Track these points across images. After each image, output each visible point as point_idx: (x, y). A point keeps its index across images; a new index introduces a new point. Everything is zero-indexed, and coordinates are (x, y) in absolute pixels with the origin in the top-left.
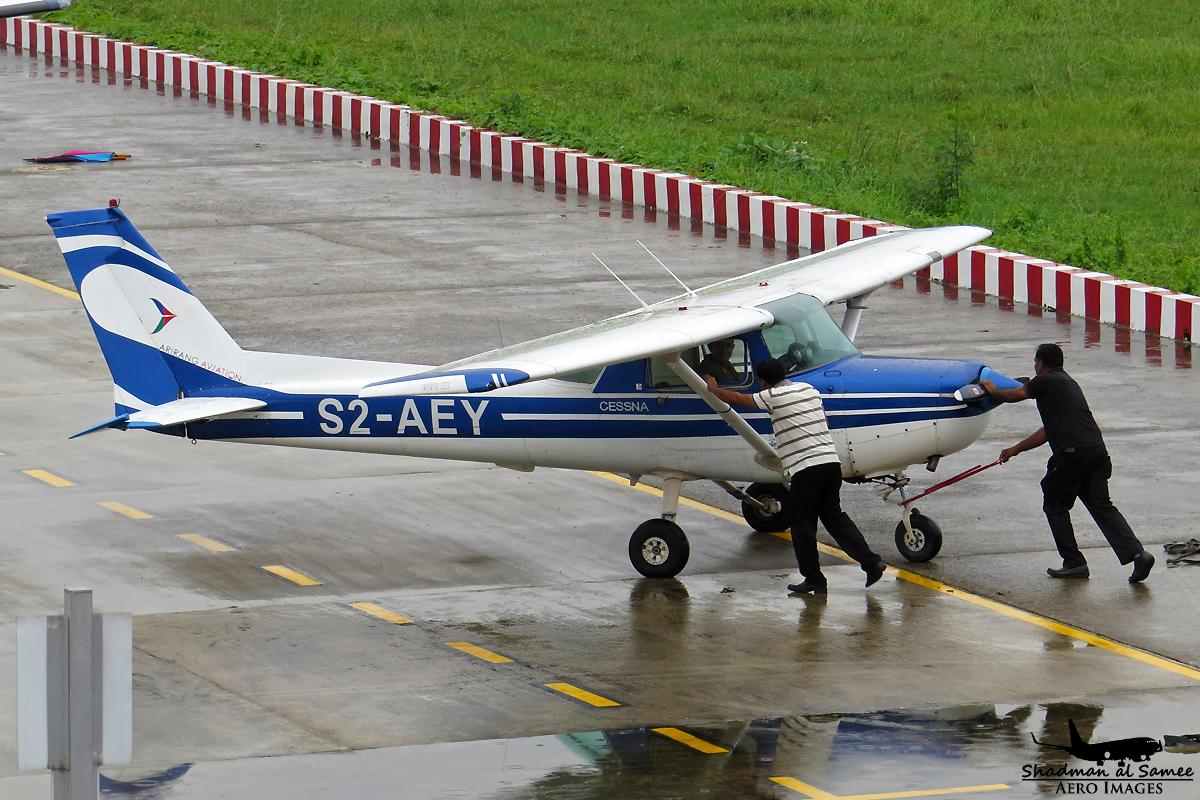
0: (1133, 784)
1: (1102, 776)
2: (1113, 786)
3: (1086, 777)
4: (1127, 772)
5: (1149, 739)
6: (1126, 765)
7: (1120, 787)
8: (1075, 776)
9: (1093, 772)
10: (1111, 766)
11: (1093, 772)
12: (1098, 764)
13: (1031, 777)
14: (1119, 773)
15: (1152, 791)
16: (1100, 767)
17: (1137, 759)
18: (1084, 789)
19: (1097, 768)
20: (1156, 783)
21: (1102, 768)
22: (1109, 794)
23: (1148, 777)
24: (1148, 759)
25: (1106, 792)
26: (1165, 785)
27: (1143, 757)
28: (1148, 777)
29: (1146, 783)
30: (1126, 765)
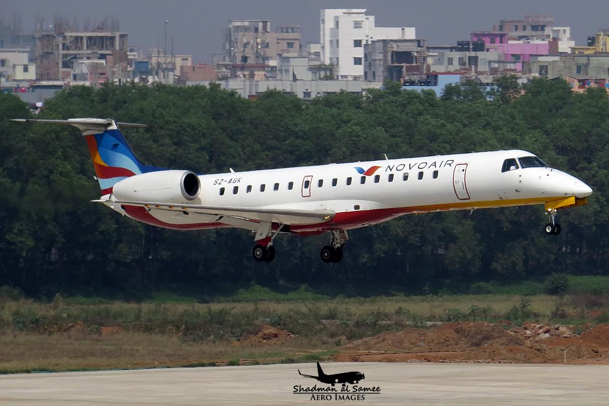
1: (334, 392)
2: (340, 396)
3: (326, 392)
4: (347, 389)
6: (346, 386)
8: (320, 391)
9: (329, 390)
10: (338, 386)
11: (329, 390)
12: (332, 385)
13: (298, 392)
15: (359, 399)
16: (333, 387)
17: (352, 383)
18: (325, 398)
20: (362, 394)
21: (334, 387)
23: (357, 392)
24: (357, 383)
25: (336, 399)
27: (355, 382)
28: (357, 392)
29: (356, 395)
30: (346, 386)
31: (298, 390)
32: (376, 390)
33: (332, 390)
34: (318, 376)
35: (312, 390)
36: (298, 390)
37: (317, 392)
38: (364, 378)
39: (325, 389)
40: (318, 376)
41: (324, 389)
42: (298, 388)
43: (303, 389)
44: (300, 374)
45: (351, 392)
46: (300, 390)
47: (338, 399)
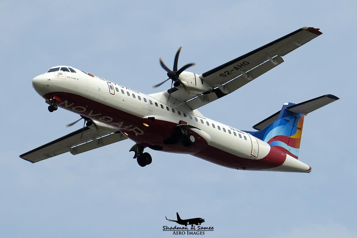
0: (196, 232)
1: (186, 230)
2: (190, 232)
3: (182, 230)
5: (201, 218)
6: (194, 226)
7: (192, 233)
8: (178, 230)
10: (189, 227)
13: (166, 230)
14: (192, 229)
15: (201, 234)
17: (197, 224)
18: (181, 233)
19: (185, 227)
20: (203, 231)
21: (186, 227)
23: (200, 230)
24: (200, 224)
25: (188, 234)
26: (205, 232)
27: (199, 224)
28: (200, 230)
29: (200, 231)
30: (194, 226)
31: (165, 229)
32: (211, 229)
34: (177, 220)
35: (173, 229)
36: (165, 229)
37: (177, 230)
38: (204, 222)
39: (181, 228)
40: (177, 220)
41: (180, 228)
42: (166, 228)
43: (168, 228)
44: (167, 219)
46: (167, 229)
47: (189, 234)
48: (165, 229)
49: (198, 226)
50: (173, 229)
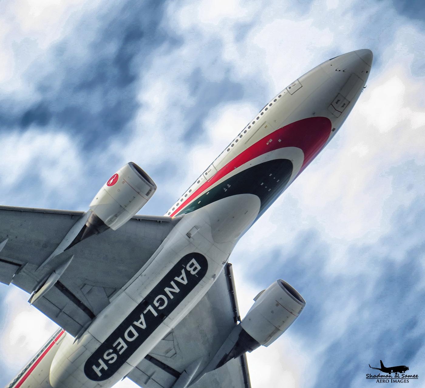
1: (390, 378)
2: (394, 381)
3: (385, 378)
4: (398, 376)
6: (398, 374)
8: (382, 378)
9: (388, 376)
10: (393, 374)
11: (388, 376)
13: (369, 378)
14: (396, 376)
15: (405, 382)
16: (390, 375)
17: (401, 372)
18: (385, 381)
20: (407, 379)
22: (393, 383)
24: (404, 372)
25: (392, 382)
26: (410, 380)
27: (403, 372)
28: (404, 378)
29: (404, 379)
30: (398, 374)
33: (390, 376)
34: (381, 368)
35: (377, 377)
37: (380, 378)
38: (408, 369)
39: (385, 376)
40: (381, 368)
41: (384, 376)
42: (369, 376)
43: (372, 376)
44: (370, 366)
45: (401, 378)
47: (393, 382)
48: (369, 377)
49: (402, 374)
50: (377, 377)
